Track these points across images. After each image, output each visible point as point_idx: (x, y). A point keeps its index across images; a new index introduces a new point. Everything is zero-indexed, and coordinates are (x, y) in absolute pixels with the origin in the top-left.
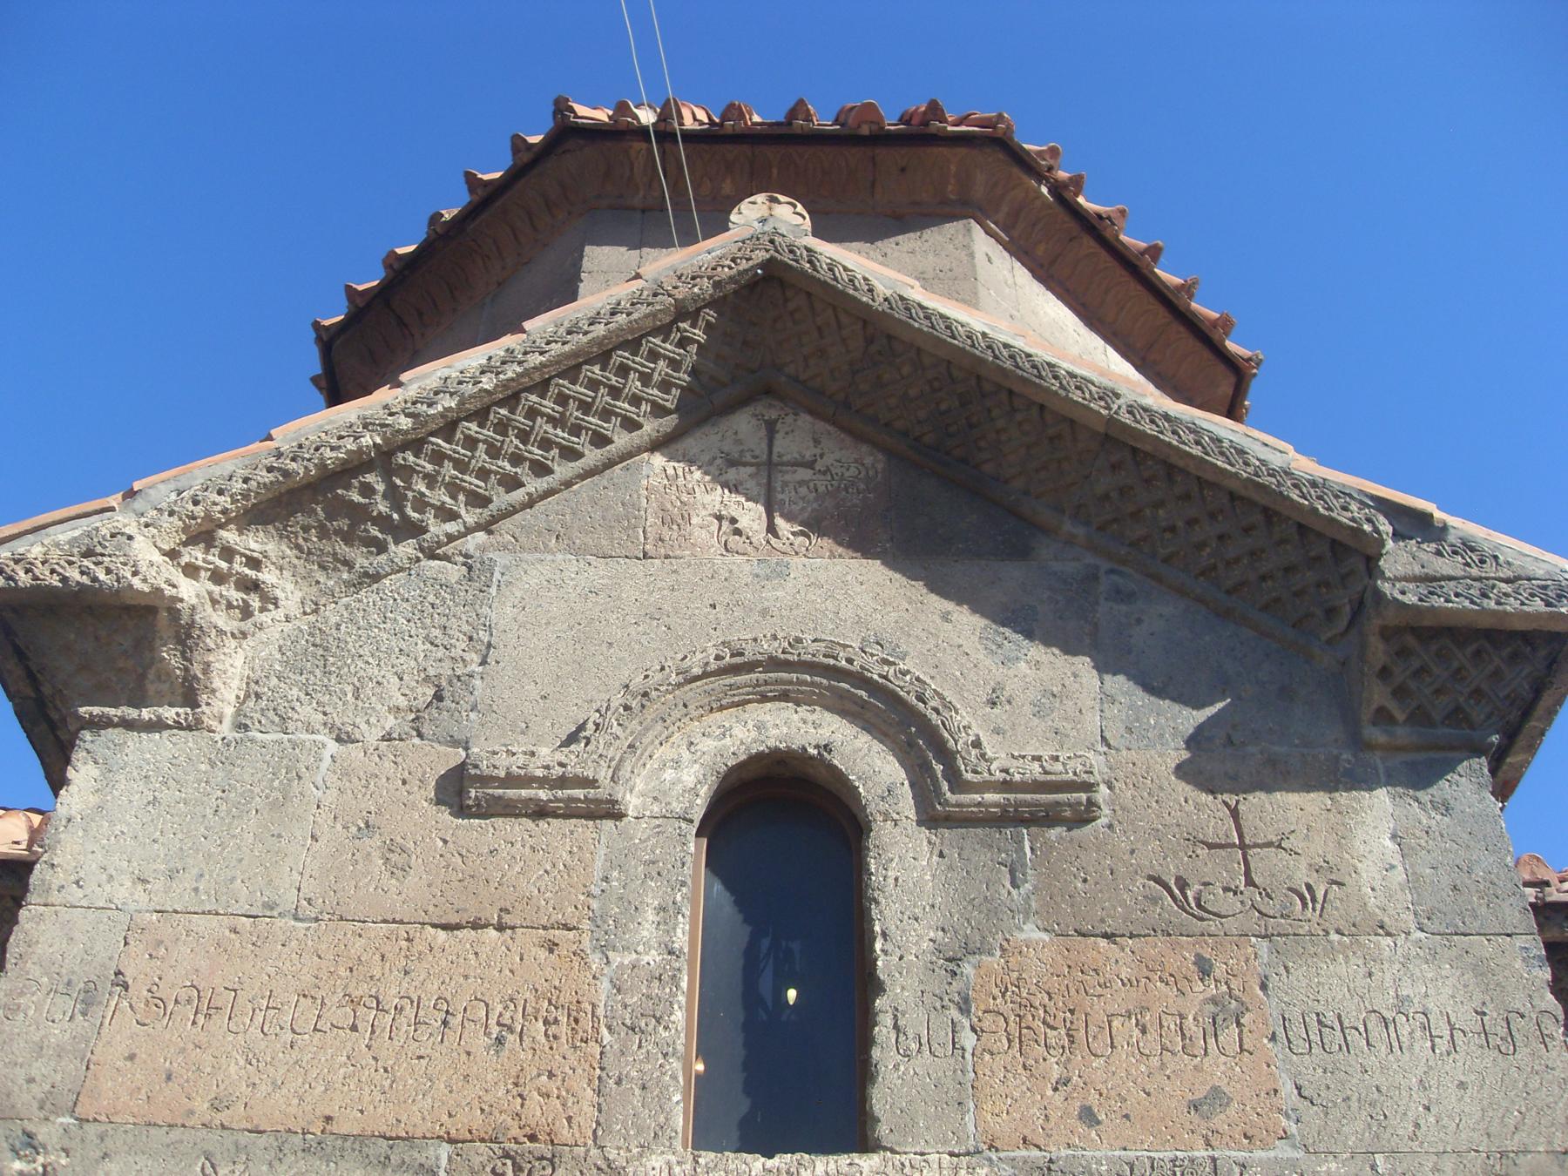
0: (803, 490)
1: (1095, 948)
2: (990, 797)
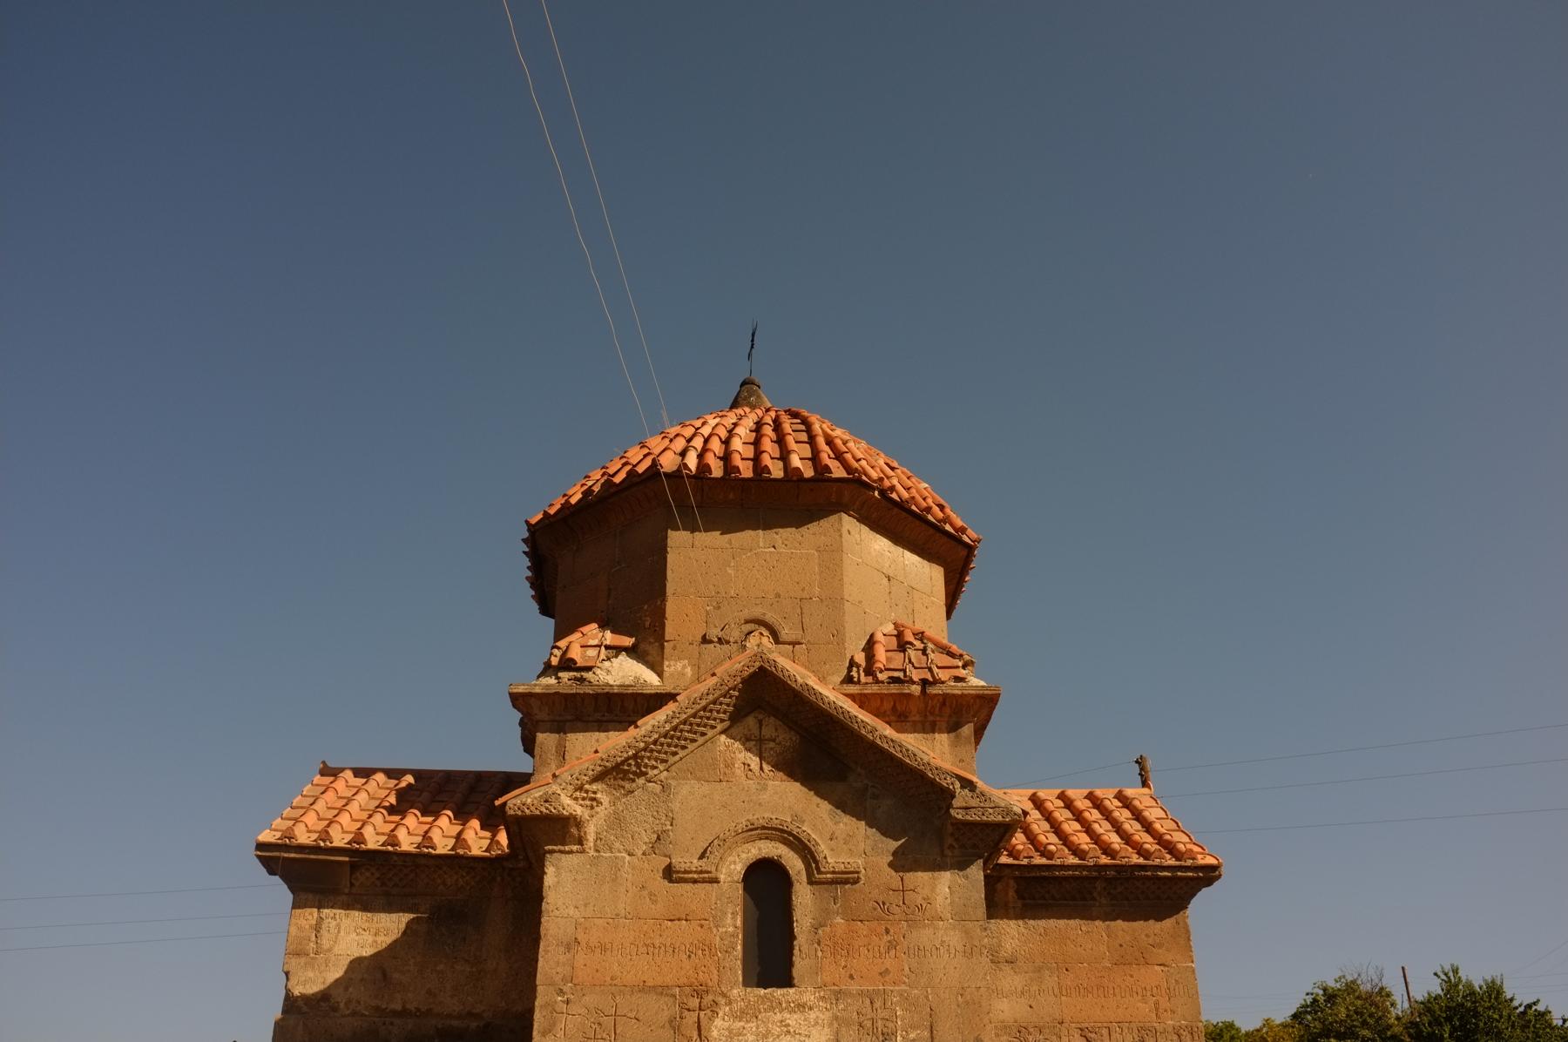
2: (829, 876)
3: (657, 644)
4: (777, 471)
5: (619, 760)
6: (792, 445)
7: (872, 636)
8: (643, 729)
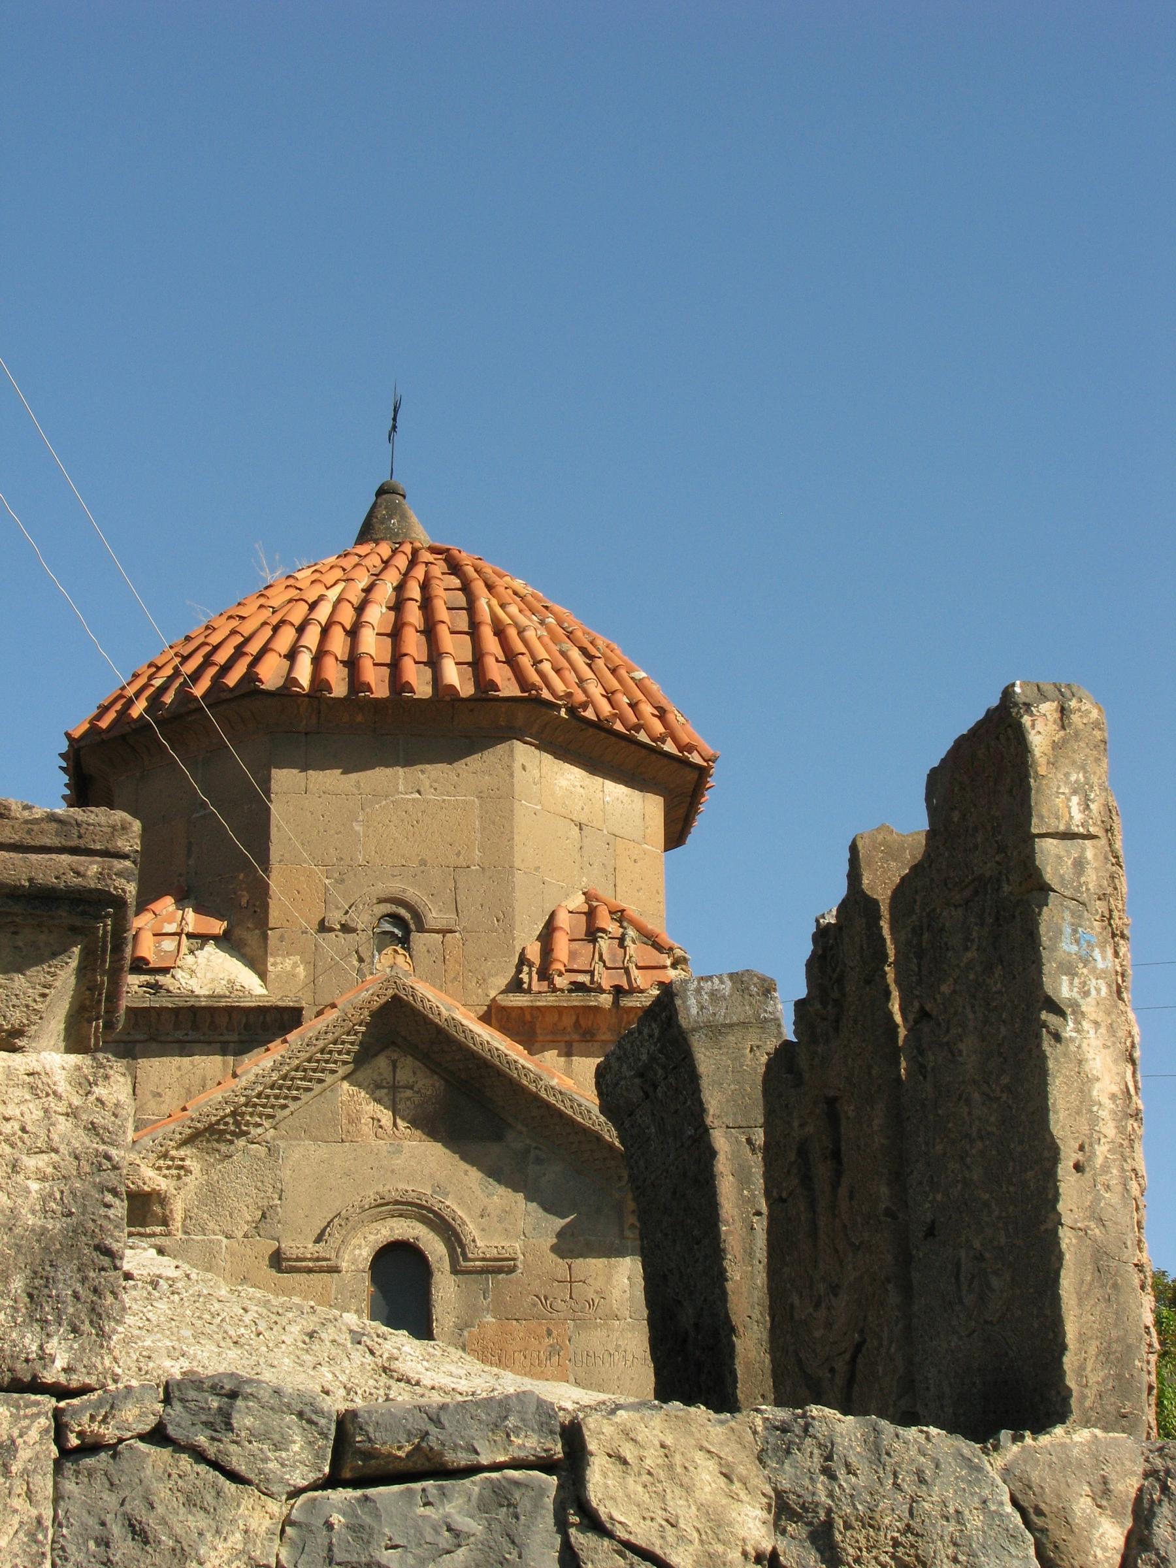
0: (408, 1103)
1: (512, 1325)
3: (257, 931)
4: (423, 690)
5: (214, 1119)
6: (447, 641)
7: (553, 915)
8: (244, 1079)
